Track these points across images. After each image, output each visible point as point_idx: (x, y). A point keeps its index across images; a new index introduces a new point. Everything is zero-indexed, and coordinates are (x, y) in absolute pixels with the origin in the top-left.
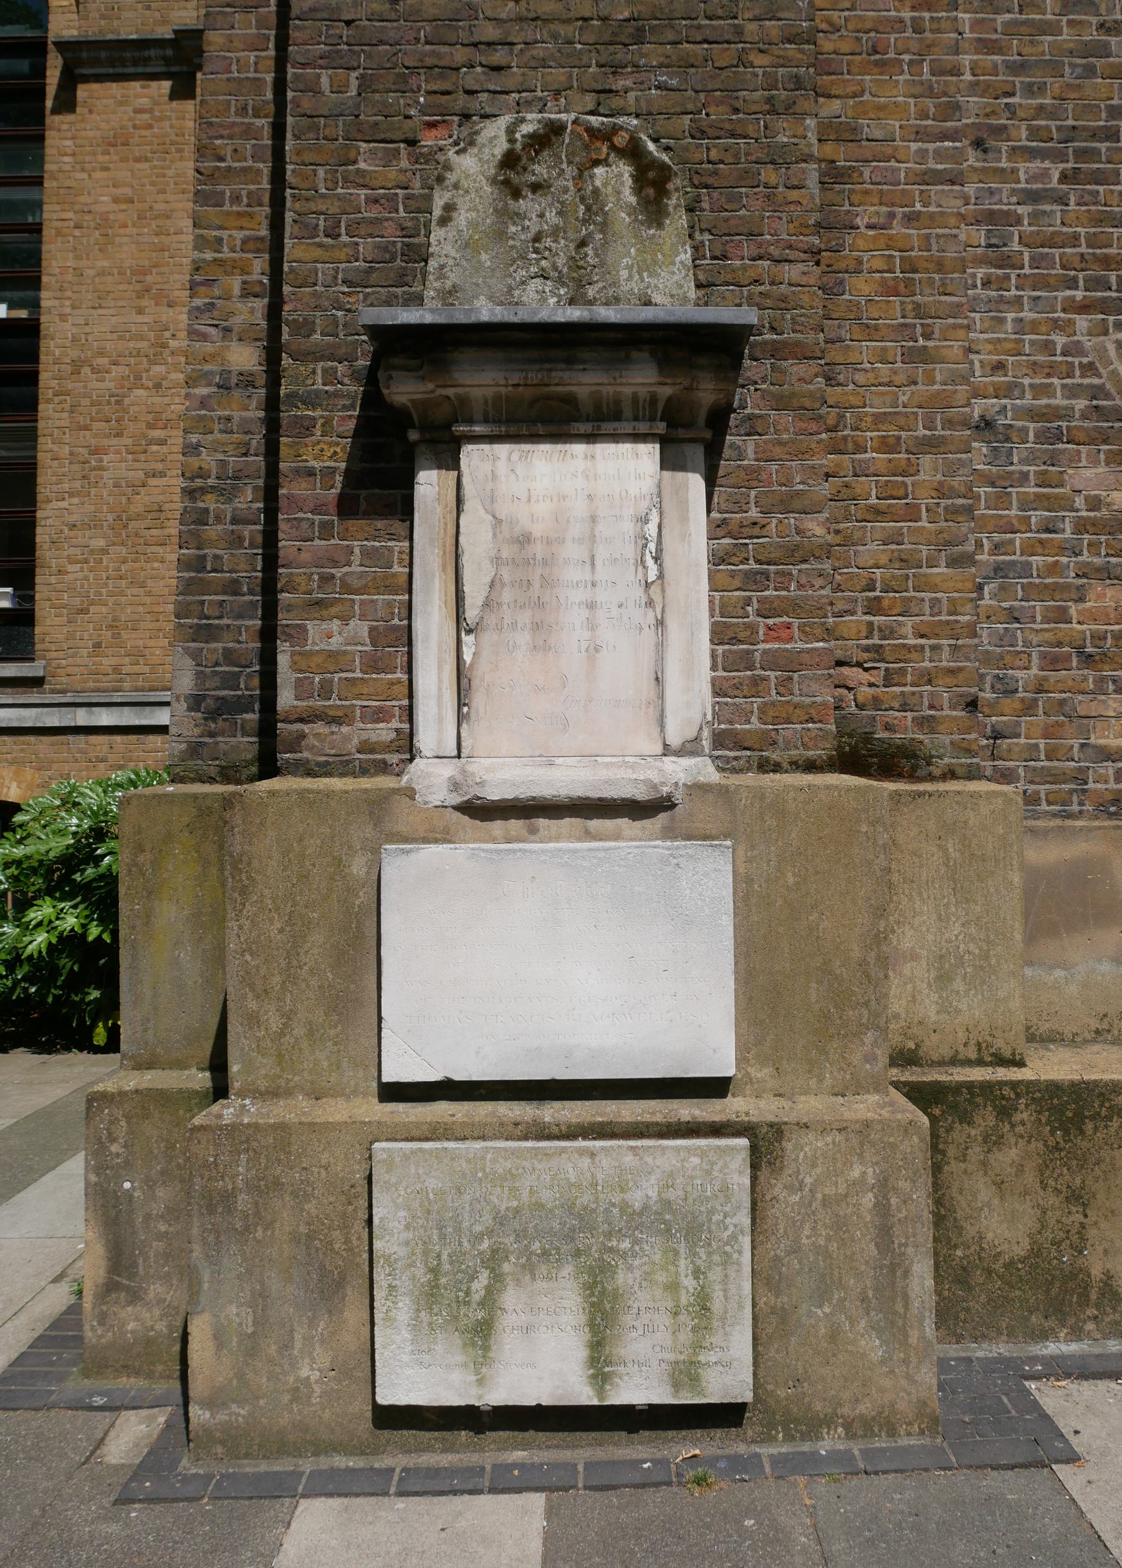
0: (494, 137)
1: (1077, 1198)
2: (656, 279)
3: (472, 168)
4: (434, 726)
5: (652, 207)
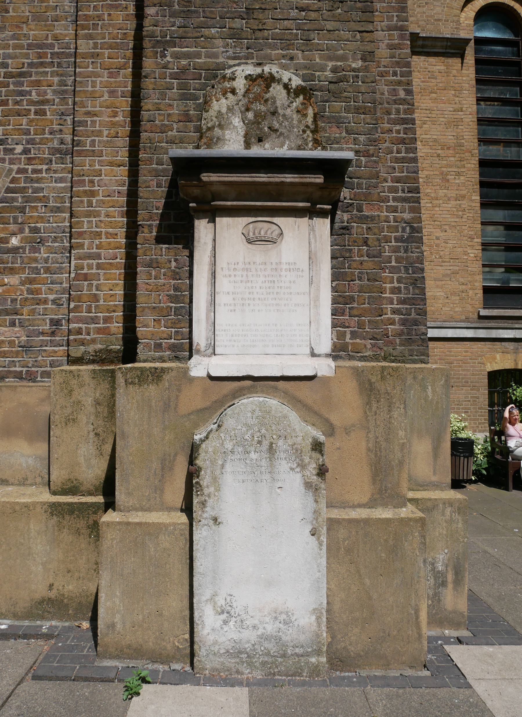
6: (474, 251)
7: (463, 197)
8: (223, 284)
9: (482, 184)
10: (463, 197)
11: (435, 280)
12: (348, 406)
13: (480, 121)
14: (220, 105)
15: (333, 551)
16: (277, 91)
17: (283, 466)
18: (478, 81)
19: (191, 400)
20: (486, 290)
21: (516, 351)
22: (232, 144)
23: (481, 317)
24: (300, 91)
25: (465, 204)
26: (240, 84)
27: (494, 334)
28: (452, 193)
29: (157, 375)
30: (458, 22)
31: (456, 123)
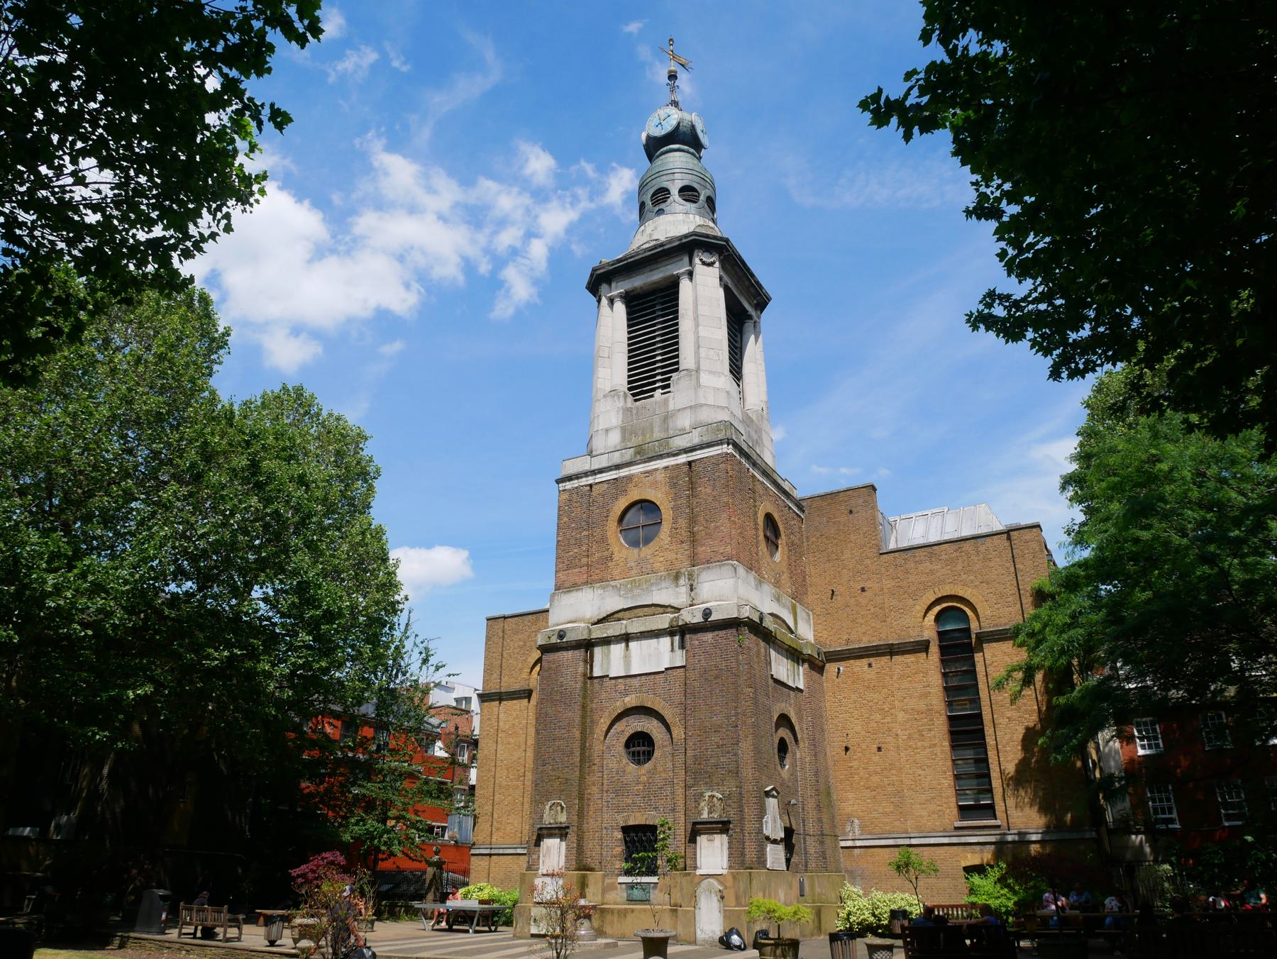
2: (563, 818)
6: (947, 781)
7: (935, 745)
9: (952, 733)
10: (935, 745)
12: (730, 882)
13: (946, 689)
14: (702, 804)
15: (725, 917)
18: (942, 661)
19: (697, 880)
20: (961, 808)
21: (982, 851)
22: (705, 816)
23: (956, 828)
27: (963, 840)
28: (926, 744)
30: (922, 627)
31: (926, 695)
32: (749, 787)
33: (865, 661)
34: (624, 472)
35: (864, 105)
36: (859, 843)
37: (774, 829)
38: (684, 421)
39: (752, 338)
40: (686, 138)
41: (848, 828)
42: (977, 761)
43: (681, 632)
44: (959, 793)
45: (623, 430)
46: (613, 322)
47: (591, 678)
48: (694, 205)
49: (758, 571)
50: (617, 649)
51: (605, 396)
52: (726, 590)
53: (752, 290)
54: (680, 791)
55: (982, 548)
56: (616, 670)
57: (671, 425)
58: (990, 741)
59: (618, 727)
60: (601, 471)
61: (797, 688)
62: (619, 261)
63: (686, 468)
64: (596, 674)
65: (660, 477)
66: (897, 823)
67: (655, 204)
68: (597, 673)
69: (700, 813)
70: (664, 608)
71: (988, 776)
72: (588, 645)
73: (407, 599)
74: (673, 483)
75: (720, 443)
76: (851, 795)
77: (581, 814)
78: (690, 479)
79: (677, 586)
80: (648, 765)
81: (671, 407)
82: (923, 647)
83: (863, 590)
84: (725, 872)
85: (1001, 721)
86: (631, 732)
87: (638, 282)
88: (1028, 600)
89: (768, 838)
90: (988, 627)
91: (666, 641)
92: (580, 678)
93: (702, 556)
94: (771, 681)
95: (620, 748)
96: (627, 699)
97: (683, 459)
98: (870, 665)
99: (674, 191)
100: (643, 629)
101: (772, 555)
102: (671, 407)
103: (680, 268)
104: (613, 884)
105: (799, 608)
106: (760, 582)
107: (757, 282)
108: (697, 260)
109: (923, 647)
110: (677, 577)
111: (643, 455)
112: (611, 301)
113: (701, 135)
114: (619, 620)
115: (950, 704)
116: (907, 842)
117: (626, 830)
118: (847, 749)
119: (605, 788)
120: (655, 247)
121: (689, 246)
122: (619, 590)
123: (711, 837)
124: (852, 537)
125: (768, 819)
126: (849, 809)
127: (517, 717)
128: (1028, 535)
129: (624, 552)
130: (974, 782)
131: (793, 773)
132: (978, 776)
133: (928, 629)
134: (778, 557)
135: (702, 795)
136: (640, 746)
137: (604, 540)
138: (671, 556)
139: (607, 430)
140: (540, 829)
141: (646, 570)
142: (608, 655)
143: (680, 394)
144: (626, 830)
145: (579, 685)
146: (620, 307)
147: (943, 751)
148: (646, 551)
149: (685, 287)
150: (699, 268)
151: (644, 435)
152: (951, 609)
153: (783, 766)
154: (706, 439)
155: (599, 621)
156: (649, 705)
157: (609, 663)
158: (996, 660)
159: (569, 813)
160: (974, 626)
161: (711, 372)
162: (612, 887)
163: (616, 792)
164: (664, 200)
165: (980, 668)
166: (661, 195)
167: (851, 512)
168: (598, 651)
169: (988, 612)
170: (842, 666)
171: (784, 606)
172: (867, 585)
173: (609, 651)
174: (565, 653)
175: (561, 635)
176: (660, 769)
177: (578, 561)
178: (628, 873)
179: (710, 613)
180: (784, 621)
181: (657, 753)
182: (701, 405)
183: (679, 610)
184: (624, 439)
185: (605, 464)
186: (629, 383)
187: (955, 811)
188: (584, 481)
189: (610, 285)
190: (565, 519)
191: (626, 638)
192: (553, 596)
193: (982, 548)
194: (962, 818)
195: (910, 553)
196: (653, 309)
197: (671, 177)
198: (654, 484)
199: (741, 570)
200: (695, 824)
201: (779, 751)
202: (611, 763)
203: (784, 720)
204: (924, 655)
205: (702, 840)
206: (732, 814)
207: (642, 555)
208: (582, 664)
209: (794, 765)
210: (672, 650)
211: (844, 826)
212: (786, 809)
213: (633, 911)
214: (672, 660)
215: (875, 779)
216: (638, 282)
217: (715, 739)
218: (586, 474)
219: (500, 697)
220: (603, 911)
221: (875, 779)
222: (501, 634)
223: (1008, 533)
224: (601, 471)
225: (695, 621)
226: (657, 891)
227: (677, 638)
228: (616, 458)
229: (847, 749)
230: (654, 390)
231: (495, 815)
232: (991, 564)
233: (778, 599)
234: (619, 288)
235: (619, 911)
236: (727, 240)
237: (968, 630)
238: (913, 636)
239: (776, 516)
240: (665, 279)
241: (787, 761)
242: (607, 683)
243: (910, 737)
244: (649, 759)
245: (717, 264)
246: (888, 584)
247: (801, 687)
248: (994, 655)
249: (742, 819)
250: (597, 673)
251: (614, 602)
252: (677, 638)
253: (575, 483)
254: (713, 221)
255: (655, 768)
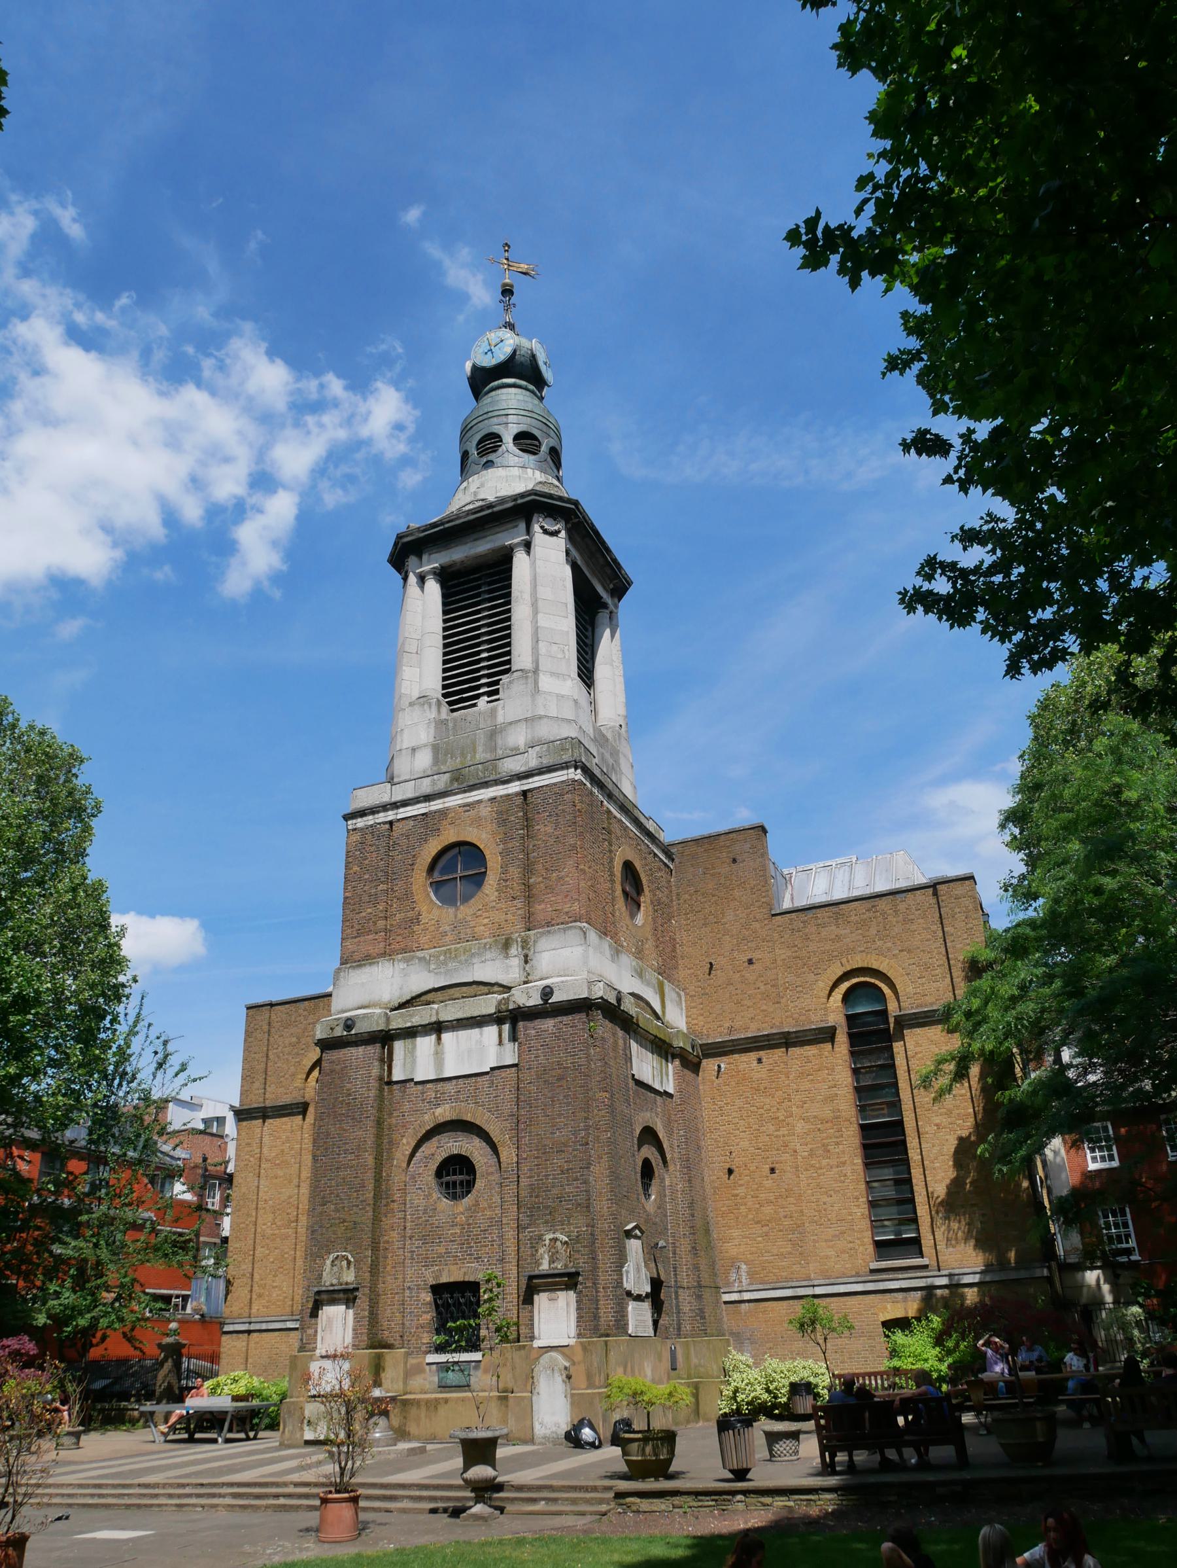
0: (331, 1257)
1: (405, 1418)
2: (349, 1277)
3: (328, 1262)
4: (319, 1345)
5: (348, 1268)
6: (860, 1210)
7: (844, 1163)
8: (542, 1315)
9: (865, 1147)
10: (844, 1163)
11: (826, 1241)
12: (579, 1355)
13: (858, 1090)
14: (541, 1251)
15: (572, 1404)
16: (558, 1243)
17: (557, 1374)
18: (852, 1053)
19: (534, 1355)
20: (878, 1245)
21: (905, 1300)
22: (545, 1267)
23: (873, 1271)
24: (566, 1243)
25: (848, 1169)
26: (547, 1242)
28: (834, 1162)
29: (524, 1346)
31: (832, 1098)
32: (603, 1225)
33: (753, 1056)
34: (436, 805)
35: (793, 237)
36: (747, 1296)
37: (637, 1280)
38: (518, 737)
39: (608, 632)
40: (523, 370)
41: (733, 1276)
42: (897, 1182)
43: (513, 1018)
44: (876, 1225)
45: (436, 749)
46: (424, 605)
47: (390, 1083)
48: (532, 457)
49: (614, 936)
50: (425, 1043)
51: (411, 704)
52: (573, 962)
53: (609, 572)
54: (511, 1234)
55: (902, 907)
56: (424, 1071)
57: (499, 742)
58: (914, 1155)
59: (426, 1149)
60: (405, 803)
61: (665, 1092)
62: (434, 525)
63: (520, 800)
64: (395, 1079)
65: (485, 811)
66: (796, 1268)
67: (482, 454)
68: (397, 1076)
69: (538, 1263)
70: (489, 987)
71: (912, 1201)
72: (385, 1039)
73: (136, 981)
74: (502, 819)
75: (565, 766)
76: (735, 1233)
77: (375, 1270)
78: (525, 814)
79: (507, 957)
80: (467, 1201)
81: (500, 719)
82: (827, 1035)
83: (750, 962)
84: (572, 1342)
85: (926, 1128)
86: (445, 1155)
87: (458, 554)
88: (958, 974)
89: (629, 1294)
90: (910, 1007)
91: (491, 1031)
92: (374, 1084)
93: (540, 917)
94: (631, 1083)
95: (429, 1177)
96: (439, 1111)
97: (515, 787)
98: (760, 1061)
99: (508, 439)
100: (460, 1015)
101: (633, 916)
102: (500, 719)
103: (514, 537)
104: (419, 1364)
105: (668, 987)
106: (618, 952)
107: (615, 561)
108: (536, 528)
109: (827, 1035)
110: (506, 945)
111: (462, 782)
112: (422, 579)
113: (543, 368)
114: (428, 1003)
115: (862, 1109)
116: (809, 1291)
117: (437, 1289)
118: (730, 1172)
119: (409, 1232)
120: (481, 509)
121: (526, 509)
122: (429, 963)
123: (553, 1295)
124: (736, 893)
125: (630, 1267)
126: (734, 1252)
127: (288, 1140)
128: (959, 889)
129: (436, 912)
130: (894, 1209)
131: (661, 1206)
132: (900, 1202)
133: (833, 1012)
134: (640, 919)
135: (540, 1238)
136: (456, 1175)
137: (408, 895)
138: (499, 917)
139: (414, 750)
140: (318, 1293)
141: (465, 936)
142: (412, 1052)
143: (512, 702)
144: (437, 1289)
145: (373, 1093)
146: (433, 588)
147: (853, 1171)
148: (465, 911)
149: (520, 562)
150: (539, 538)
151: (463, 755)
152: (863, 987)
153: (647, 1196)
154: (546, 761)
155: (402, 1006)
156: (469, 1118)
157: (414, 1062)
158: (920, 1050)
159: (358, 1269)
160: (892, 1007)
161: (552, 674)
162: (418, 1370)
163: (424, 1239)
164: (495, 449)
165: (900, 1061)
166: (490, 442)
167: (734, 861)
168: (399, 1046)
169: (910, 989)
170: (724, 1063)
171: (648, 984)
172: (755, 956)
173: (414, 1047)
174: (353, 1050)
175: (349, 1024)
176: (483, 1204)
177: (371, 927)
178: (440, 1349)
179: (551, 993)
180: (648, 1004)
181: (479, 1184)
182: (540, 717)
183: (509, 989)
184: (436, 761)
185: (410, 795)
186: (444, 687)
187: (871, 1249)
188: (382, 817)
189: (420, 557)
190: (356, 868)
191: (438, 1028)
192: (338, 972)
193: (902, 907)
194: (880, 1257)
195: (810, 914)
196: (477, 591)
197: (504, 419)
198: (477, 822)
199: (593, 935)
200: (531, 1278)
201: (643, 1177)
202: (416, 1199)
203: (649, 1135)
204: (829, 1045)
205: (541, 1299)
206: (582, 1263)
207: (460, 916)
208: (376, 1063)
209: (661, 1195)
210: (500, 1043)
211: (727, 1273)
212: (653, 1253)
213: (446, 1401)
214: (499, 1056)
215: (768, 1210)
216: (458, 554)
217: (558, 1161)
218: (385, 808)
219: (264, 1113)
220: (405, 1403)
221: (768, 1210)
222: (266, 1027)
223: (934, 887)
224: (405, 803)
225: (531, 1003)
226: (479, 1373)
227: (506, 1027)
228: (426, 787)
229: (730, 1172)
230: (477, 697)
231: (256, 1276)
232: (914, 927)
233: (640, 974)
234: (431, 563)
235: (428, 1402)
236: (576, 503)
237: (884, 1013)
238: (816, 1021)
239: (638, 865)
240: (494, 551)
241: (653, 1190)
242: (412, 1089)
243: (812, 1153)
244: (468, 1192)
245: (563, 534)
246: (782, 953)
247: (671, 1091)
248: (917, 1044)
249: (595, 1268)
250: (397, 1076)
251: (420, 980)
252: (506, 1027)
253: (370, 820)
254: (558, 479)
255: (477, 1204)
